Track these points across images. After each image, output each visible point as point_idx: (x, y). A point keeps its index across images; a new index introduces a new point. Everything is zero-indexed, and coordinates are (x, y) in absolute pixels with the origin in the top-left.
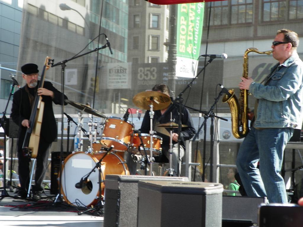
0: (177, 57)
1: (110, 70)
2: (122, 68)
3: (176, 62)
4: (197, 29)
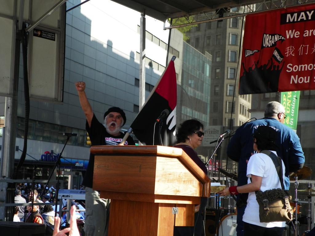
2: (215, 130)
4: (293, 105)
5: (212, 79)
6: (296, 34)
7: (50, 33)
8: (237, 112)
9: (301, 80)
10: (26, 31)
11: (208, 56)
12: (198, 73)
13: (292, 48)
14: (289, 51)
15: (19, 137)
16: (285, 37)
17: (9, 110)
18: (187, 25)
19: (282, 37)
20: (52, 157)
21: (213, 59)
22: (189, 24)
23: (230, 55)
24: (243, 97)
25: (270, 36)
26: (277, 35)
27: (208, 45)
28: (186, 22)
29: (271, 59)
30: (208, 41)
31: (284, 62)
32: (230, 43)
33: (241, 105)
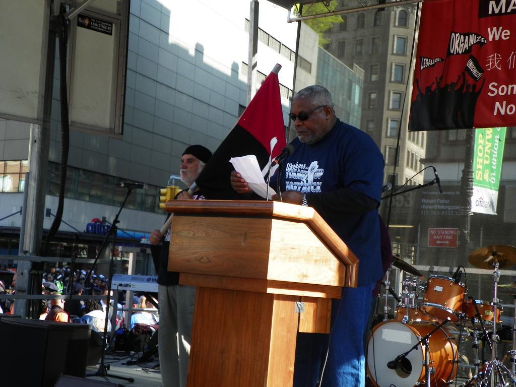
0: (474, 187)
3: (472, 193)
4: (496, 151)
5: (363, 109)
6: (503, 34)
7: (105, 22)
8: (403, 164)
9: (511, 109)
10: (66, 18)
12: (341, 99)
13: (498, 57)
14: (493, 62)
15: (51, 193)
16: (487, 38)
17: (36, 144)
18: (325, 16)
19: (481, 39)
20: (104, 227)
21: (366, 76)
22: (329, 14)
23: (393, 71)
24: (414, 140)
25: (462, 36)
26: (473, 35)
27: (360, 53)
28: (326, 10)
29: (463, 74)
30: (359, 48)
31: (484, 79)
32: (395, 52)
33: (409, 152)
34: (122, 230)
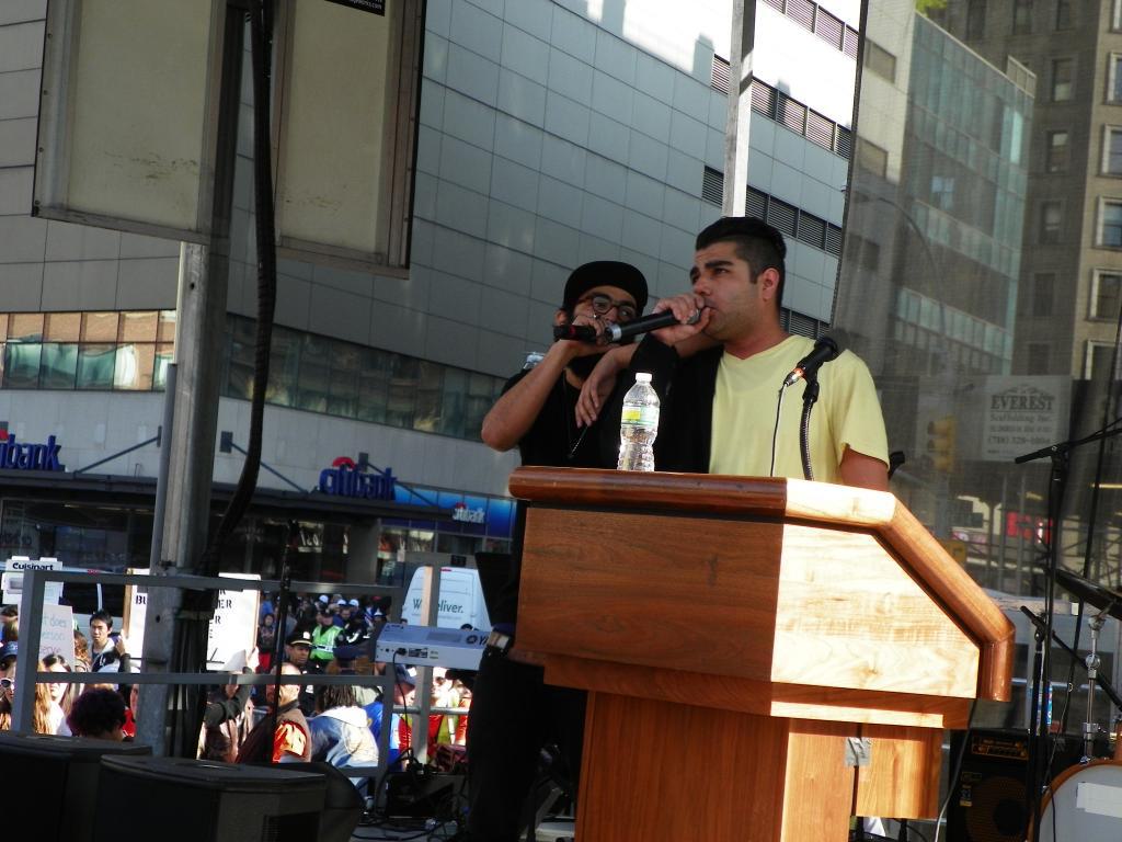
1: (995, 398)
2: (1038, 395)
11: (1021, 79)
15: (238, 394)
20: (362, 479)
21: (1040, 89)
23: (1113, 75)
27: (1027, 29)
30: (1021, 13)
34: (405, 485)
